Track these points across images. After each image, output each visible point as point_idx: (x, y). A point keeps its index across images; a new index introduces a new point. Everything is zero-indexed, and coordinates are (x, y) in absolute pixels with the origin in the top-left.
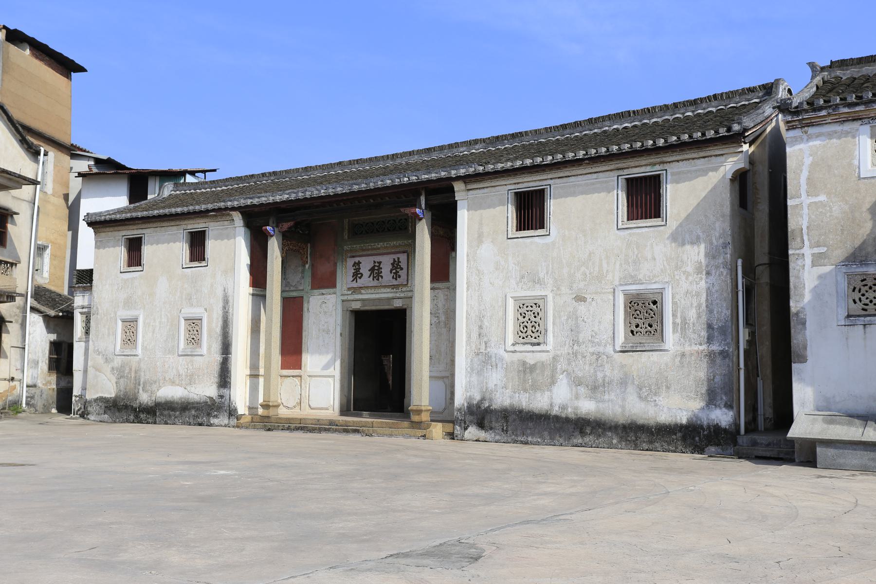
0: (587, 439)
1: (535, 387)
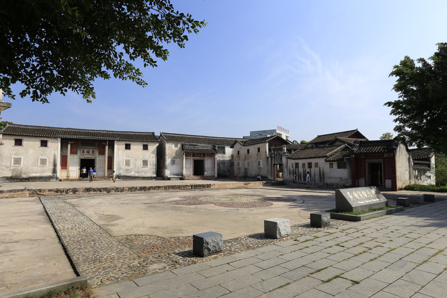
0: (137, 179)
1: (129, 172)
